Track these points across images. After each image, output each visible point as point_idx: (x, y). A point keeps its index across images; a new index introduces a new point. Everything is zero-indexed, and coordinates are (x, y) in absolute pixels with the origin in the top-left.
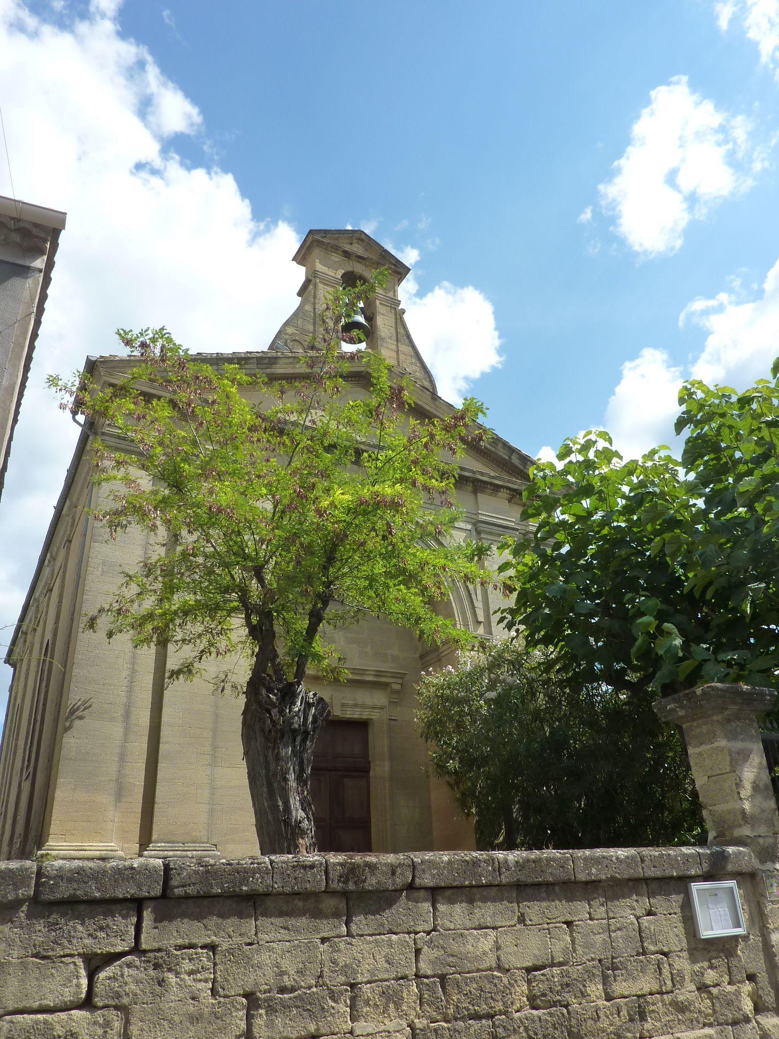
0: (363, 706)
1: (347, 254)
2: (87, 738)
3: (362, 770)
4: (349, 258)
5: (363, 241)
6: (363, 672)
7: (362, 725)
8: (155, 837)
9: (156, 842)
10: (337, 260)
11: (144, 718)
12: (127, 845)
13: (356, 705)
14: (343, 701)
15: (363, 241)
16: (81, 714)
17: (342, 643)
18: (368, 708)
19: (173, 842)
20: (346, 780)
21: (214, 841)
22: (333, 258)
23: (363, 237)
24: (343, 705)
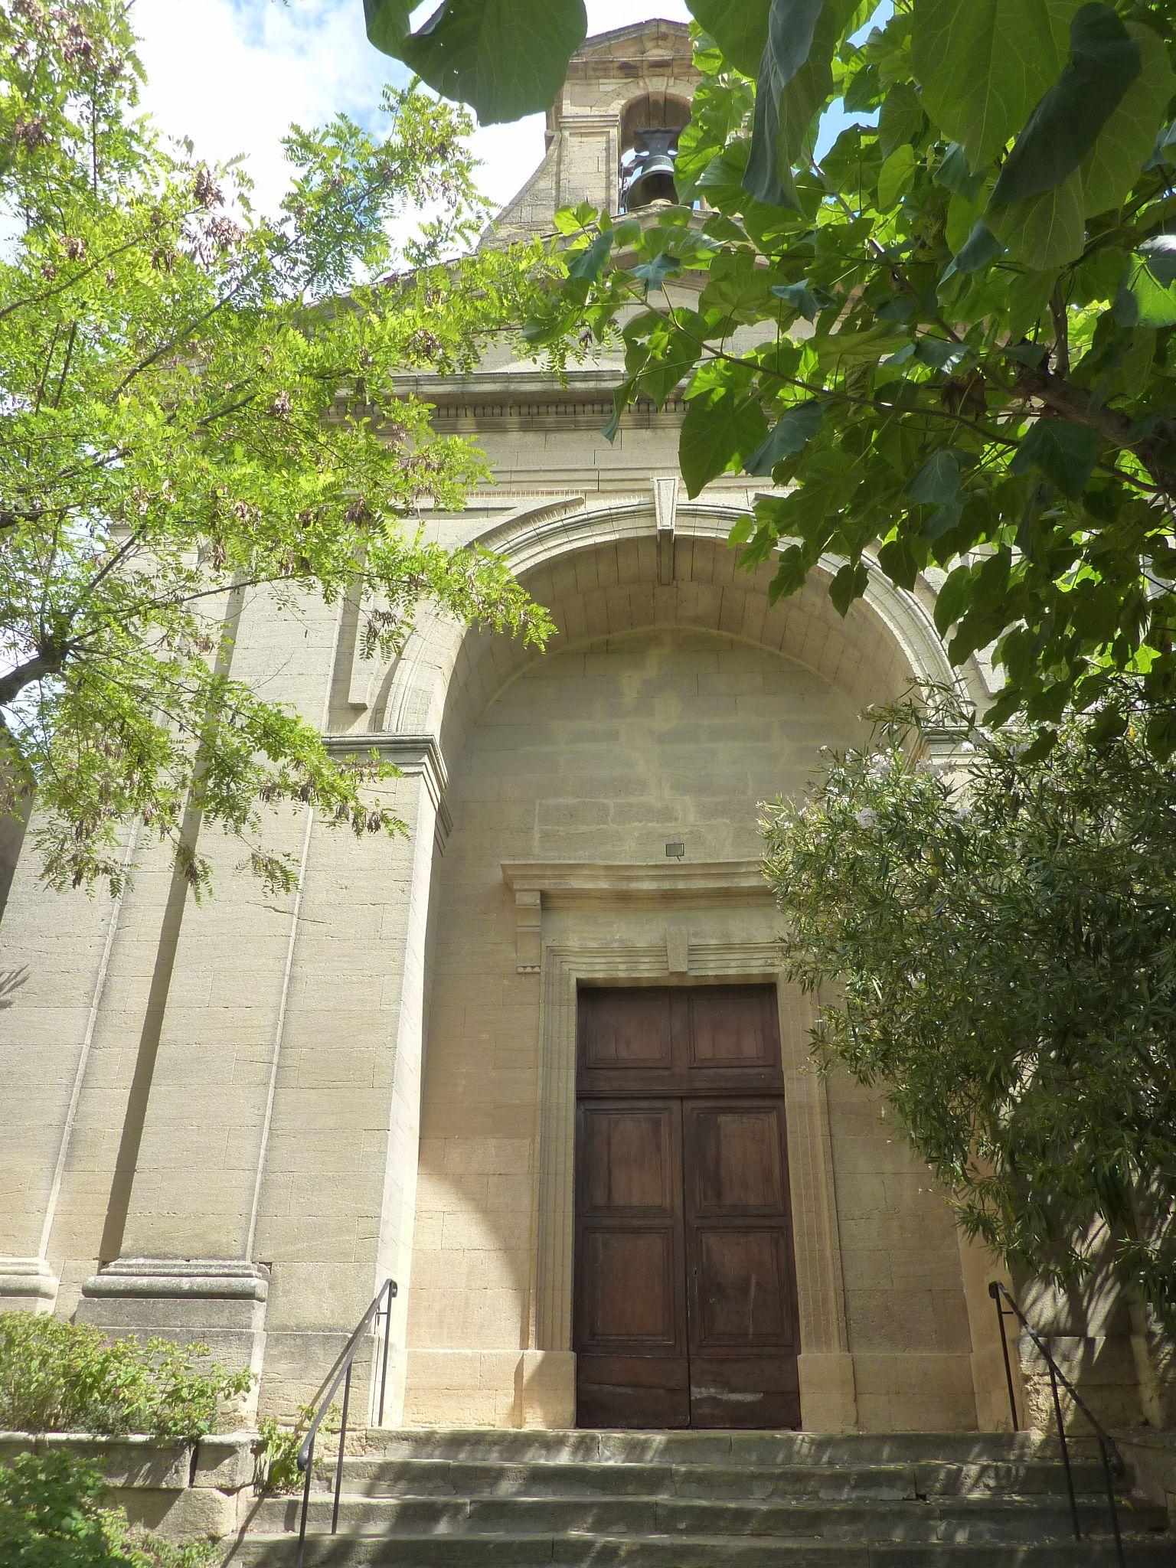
0: (747, 947)
1: (629, 71)
2: (12, 1043)
3: (766, 1094)
4: (636, 76)
5: (664, 37)
6: (730, 869)
7: (759, 993)
8: (126, 1245)
9: (128, 1256)
10: (611, 88)
11: (135, 997)
12: (73, 1264)
13: (728, 947)
14: (694, 941)
15: (664, 37)
16: (8, 997)
17: (691, 818)
18: (760, 950)
19: (165, 1257)
20: (723, 1119)
21: (266, 1256)
22: (602, 88)
23: (663, 29)
24: (693, 950)
